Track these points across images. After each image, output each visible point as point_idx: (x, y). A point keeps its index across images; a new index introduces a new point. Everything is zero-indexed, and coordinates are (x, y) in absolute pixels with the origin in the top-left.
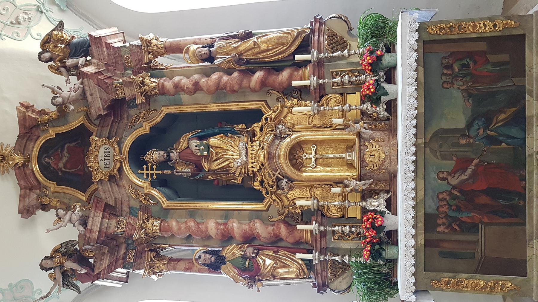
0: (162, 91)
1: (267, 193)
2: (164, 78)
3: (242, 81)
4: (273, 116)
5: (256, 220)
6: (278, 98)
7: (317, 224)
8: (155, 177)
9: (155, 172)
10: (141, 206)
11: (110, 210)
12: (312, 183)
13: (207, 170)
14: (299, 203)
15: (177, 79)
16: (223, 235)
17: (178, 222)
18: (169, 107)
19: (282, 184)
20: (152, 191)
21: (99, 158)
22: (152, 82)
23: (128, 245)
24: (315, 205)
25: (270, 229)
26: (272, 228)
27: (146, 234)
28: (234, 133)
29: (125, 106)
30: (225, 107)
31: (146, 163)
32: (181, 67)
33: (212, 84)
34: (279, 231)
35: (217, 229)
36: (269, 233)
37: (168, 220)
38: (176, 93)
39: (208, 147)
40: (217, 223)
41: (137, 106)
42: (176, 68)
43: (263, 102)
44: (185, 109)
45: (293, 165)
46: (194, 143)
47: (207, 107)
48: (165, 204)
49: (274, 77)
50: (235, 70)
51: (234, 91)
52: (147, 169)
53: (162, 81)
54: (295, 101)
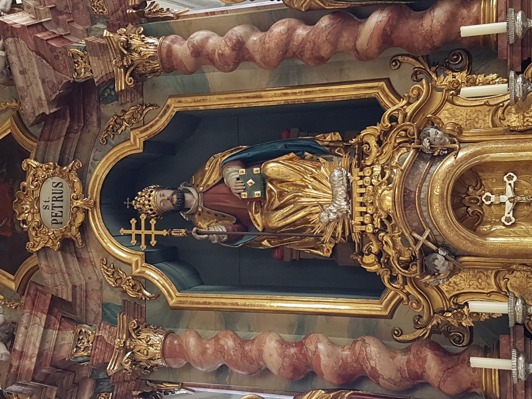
0: (168, 64)
1: (393, 279)
2: (172, 37)
3: (338, 36)
4: (409, 110)
5: (368, 339)
6: (415, 74)
7: (521, 358)
8: (153, 242)
9: (153, 232)
10: (124, 301)
11: (63, 311)
12: (505, 260)
13: (260, 229)
14: (477, 306)
15: (198, 36)
16: (295, 369)
17: (199, 337)
18: (183, 99)
20: (148, 272)
21: (42, 204)
22: (148, 46)
23: (98, 382)
24: (519, 314)
25: (401, 359)
26: (405, 358)
27: (135, 362)
28: (318, 152)
29: (94, 97)
30: (298, 96)
31: (136, 214)
32: (207, 14)
33: (272, 45)
34: (422, 367)
35: (283, 356)
36: (400, 370)
37: (180, 331)
38: (197, 68)
39: (263, 180)
40: (283, 343)
41: (117, 96)
42: (195, 15)
43: (383, 83)
44: (214, 102)
45: (461, 219)
46: (235, 173)
47: (260, 97)
48: (175, 298)
49: (411, 23)
50: (322, 12)
51: (321, 60)
52: (138, 227)
53: (167, 42)
54: (461, 76)
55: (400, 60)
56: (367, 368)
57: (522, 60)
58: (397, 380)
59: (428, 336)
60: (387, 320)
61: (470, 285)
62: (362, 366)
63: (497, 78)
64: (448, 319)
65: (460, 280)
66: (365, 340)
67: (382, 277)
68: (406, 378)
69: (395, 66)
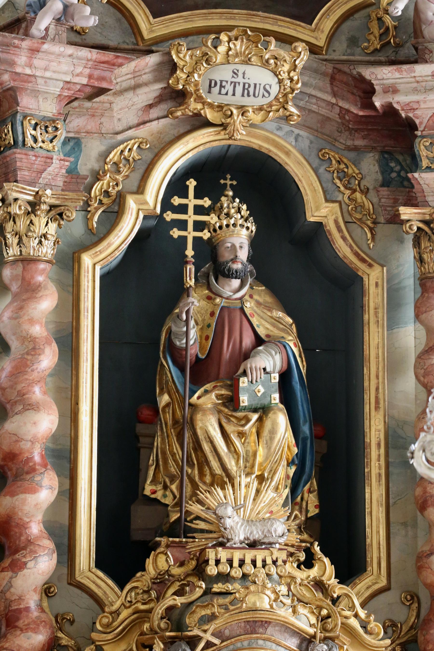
6: (394, 624)
8: (176, 233)
9: (191, 234)
21: (242, 68)
39: (263, 410)
55: (413, 605)
56: (24, 557)
58: (8, 595)
62: (25, 548)
68: (10, 606)
69: (406, 598)
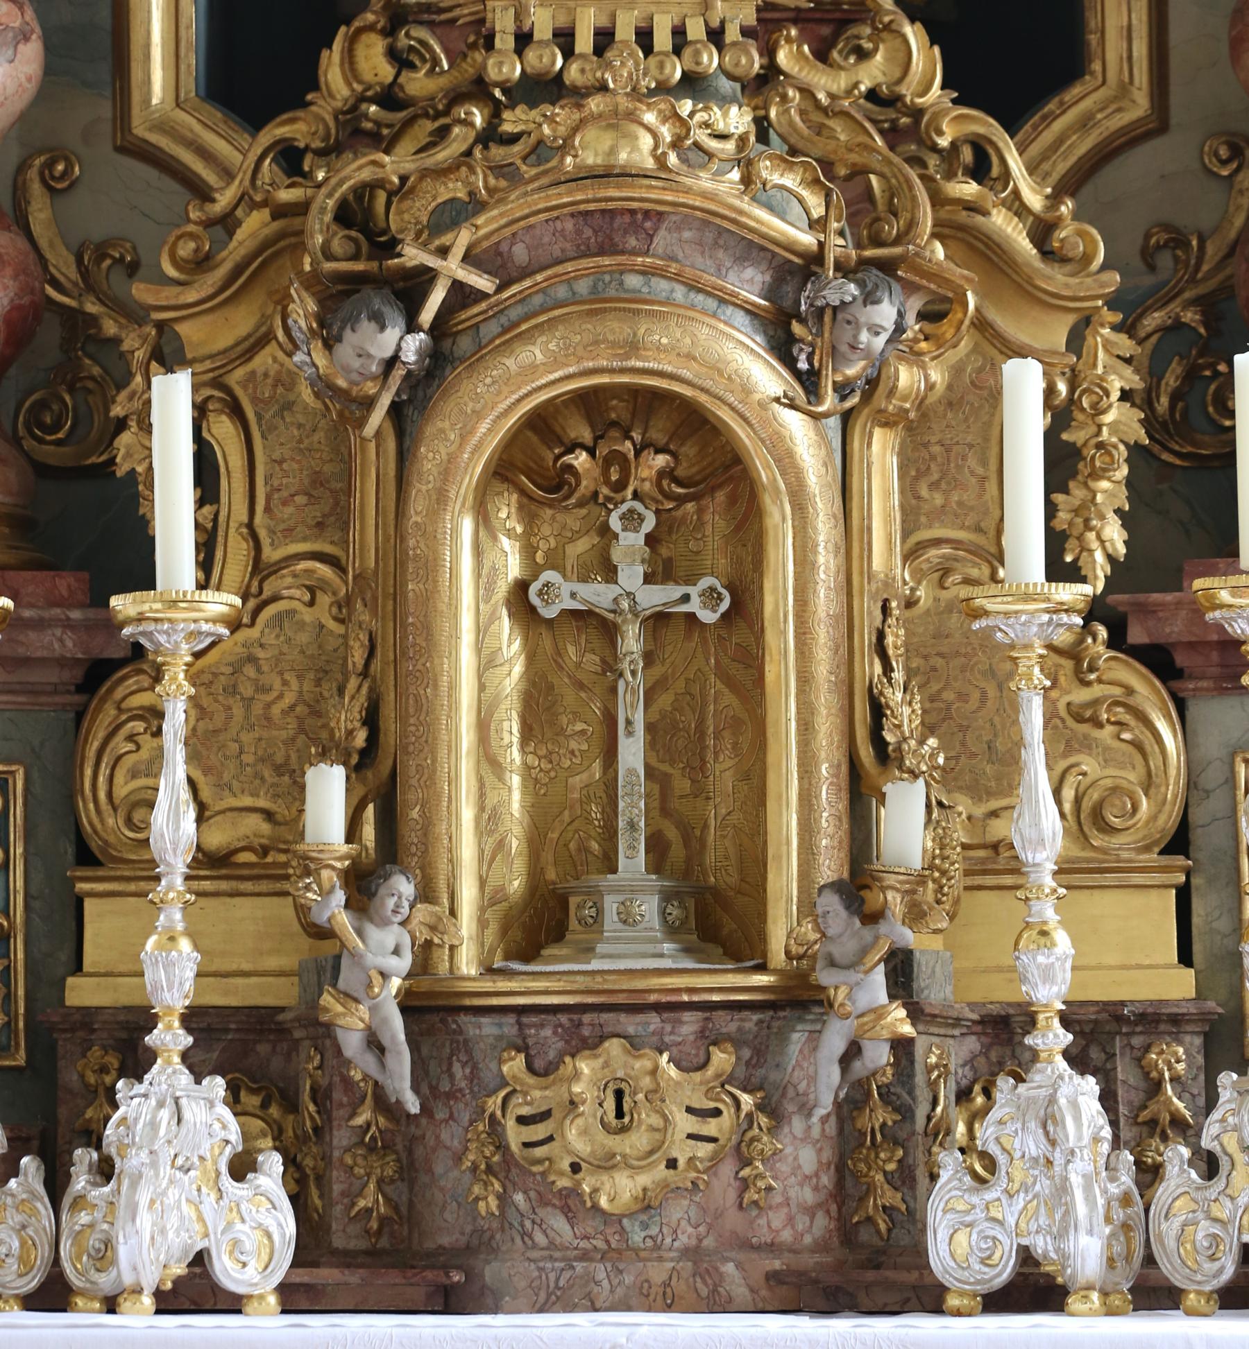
1: (290, 158)
19: (367, 327)
45: (541, 423)
57: (1173, 645)
59: (50, 300)
60: (107, 128)
61: (280, 463)
63: (1111, 558)
64: (138, 379)
65: (300, 426)
66: (27, 39)
67: (300, 113)
